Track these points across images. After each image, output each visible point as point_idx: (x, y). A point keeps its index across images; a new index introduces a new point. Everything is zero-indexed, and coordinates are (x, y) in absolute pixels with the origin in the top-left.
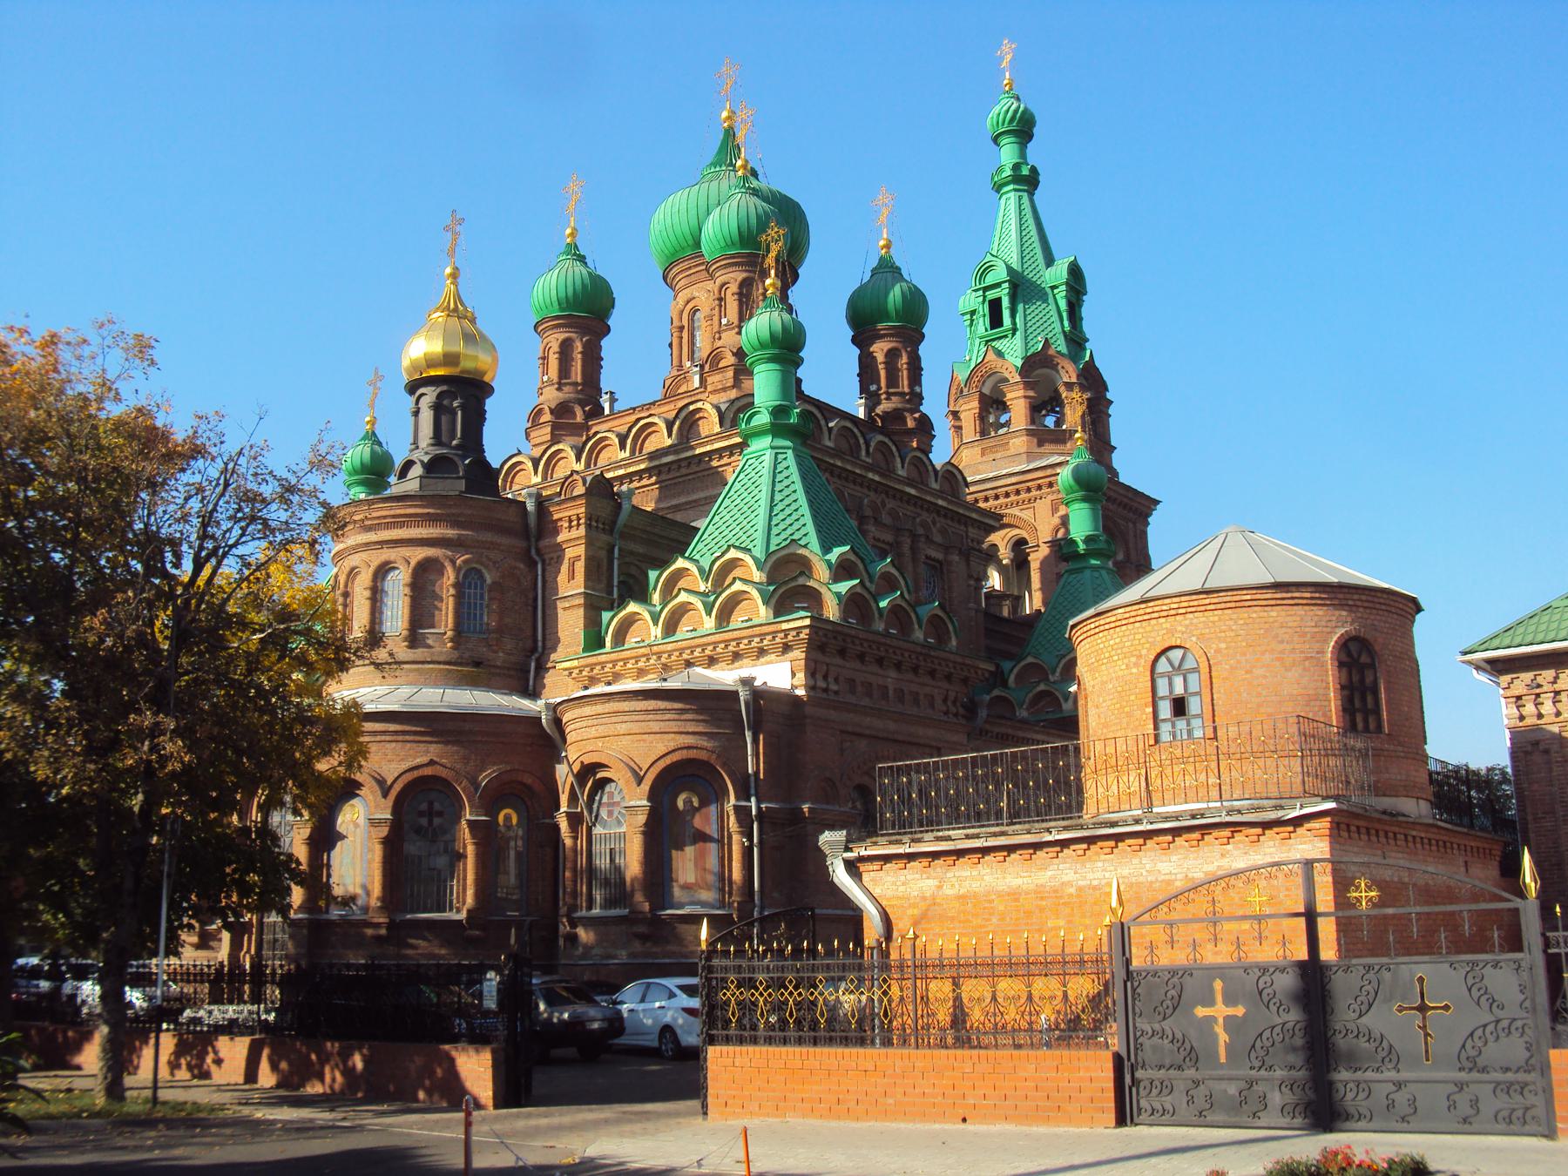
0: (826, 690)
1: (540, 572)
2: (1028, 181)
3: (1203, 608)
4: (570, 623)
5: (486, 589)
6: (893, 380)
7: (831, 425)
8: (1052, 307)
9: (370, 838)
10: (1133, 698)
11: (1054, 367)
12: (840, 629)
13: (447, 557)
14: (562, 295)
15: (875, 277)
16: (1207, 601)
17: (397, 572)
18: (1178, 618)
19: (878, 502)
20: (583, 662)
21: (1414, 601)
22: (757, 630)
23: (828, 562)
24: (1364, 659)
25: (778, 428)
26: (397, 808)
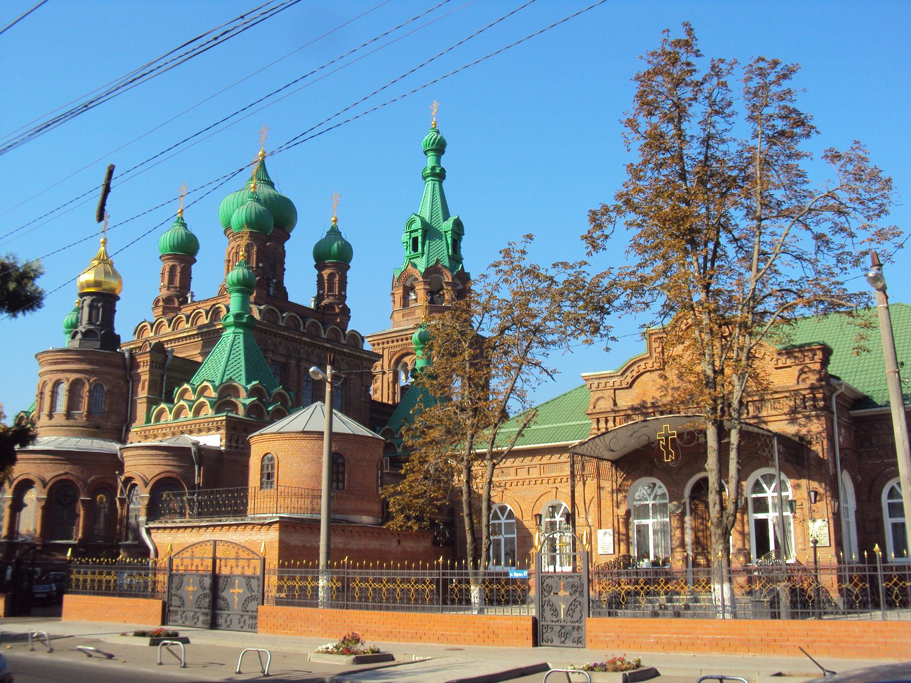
0: (237, 447)
2: (440, 175)
4: (141, 409)
6: (331, 289)
7: (284, 315)
8: (444, 242)
11: (441, 273)
13: (86, 378)
14: (172, 244)
20: (142, 429)
22: (189, 422)
23: (246, 389)
24: (340, 461)
25: (237, 324)
26: (50, 493)
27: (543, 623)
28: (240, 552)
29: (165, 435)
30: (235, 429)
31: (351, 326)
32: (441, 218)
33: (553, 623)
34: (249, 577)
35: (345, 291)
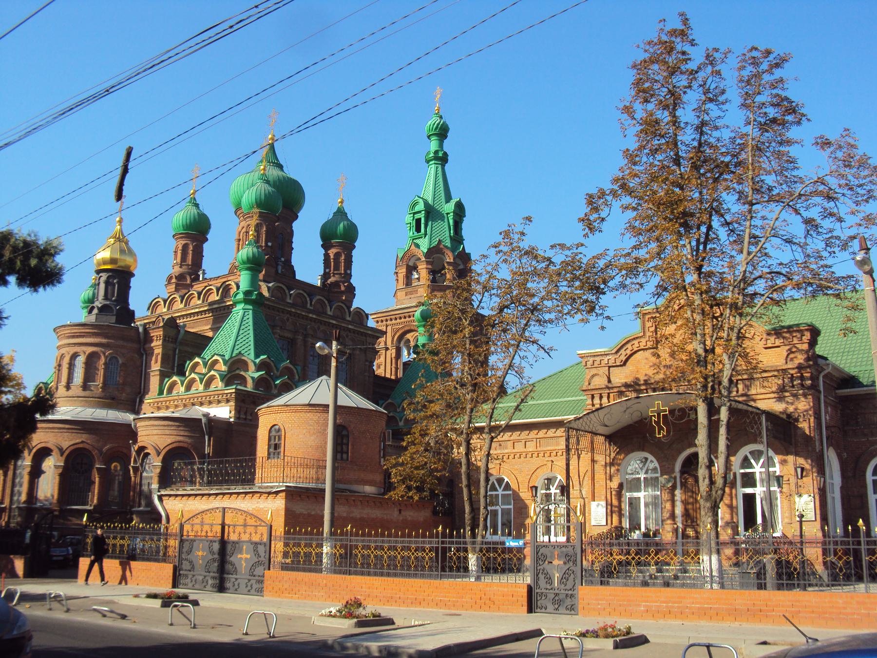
0: (245, 419)
2: (442, 159)
4: (154, 381)
6: (337, 267)
7: (292, 292)
8: (446, 223)
11: (443, 254)
13: (101, 351)
14: (184, 223)
20: (155, 400)
22: (200, 395)
23: (255, 363)
24: (344, 433)
25: (246, 301)
26: (67, 461)
27: (538, 591)
28: (248, 519)
29: (176, 406)
30: (243, 401)
31: (355, 304)
33: (547, 591)
34: (256, 543)
35: (351, 270)
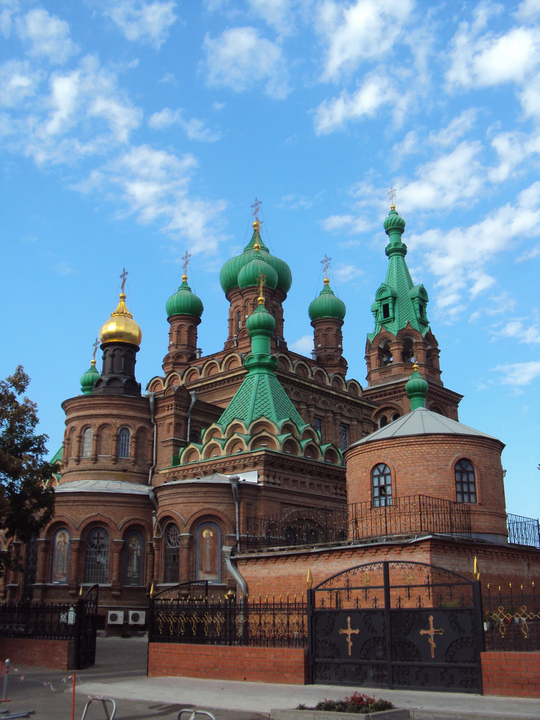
1: (155, 430)
3: (392, 446)
5: (130, 437)
9: (71, 548)
10: (363, 487)
12: (280, 456)
15: (321, 296)
16: (395, 442)
17: (91, 429)
18: (382, 450)
19: (317, 398)
20: (170, 470)
21: (497, 442)
30: (272, 464)
31: (348, 377)
32: (407, 286)
34: (453, 611)
35: (341, 344)
